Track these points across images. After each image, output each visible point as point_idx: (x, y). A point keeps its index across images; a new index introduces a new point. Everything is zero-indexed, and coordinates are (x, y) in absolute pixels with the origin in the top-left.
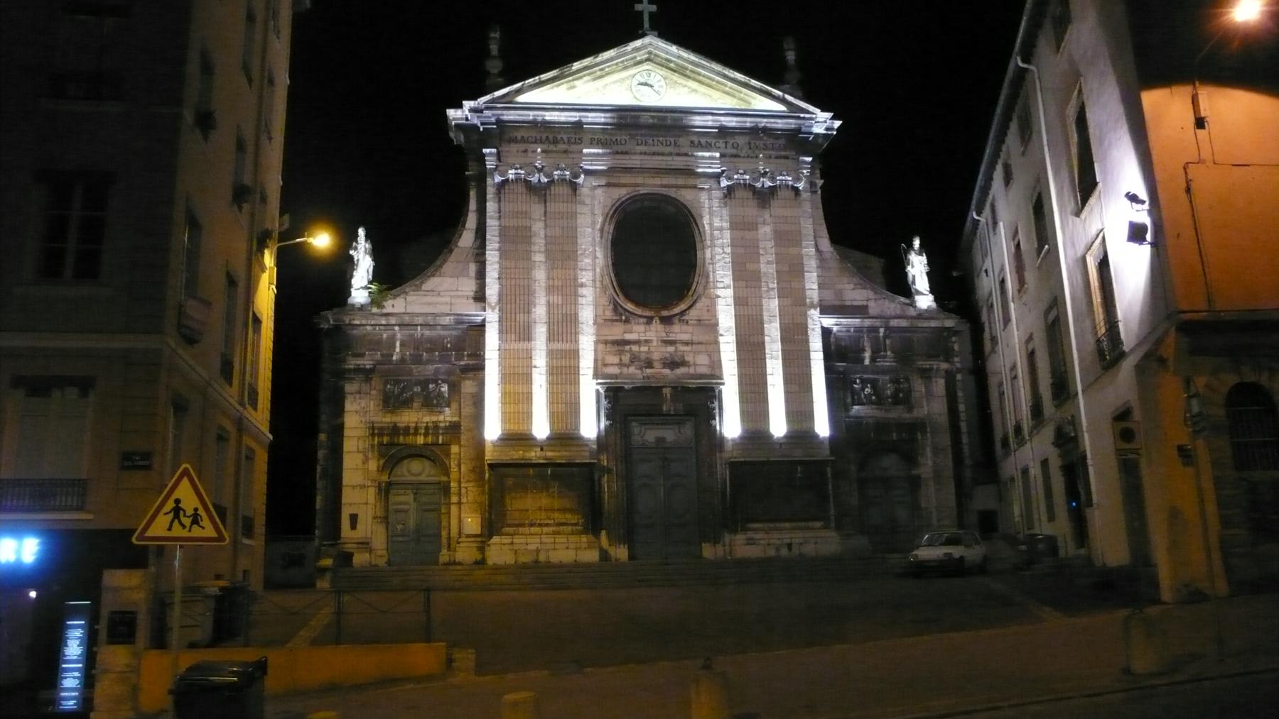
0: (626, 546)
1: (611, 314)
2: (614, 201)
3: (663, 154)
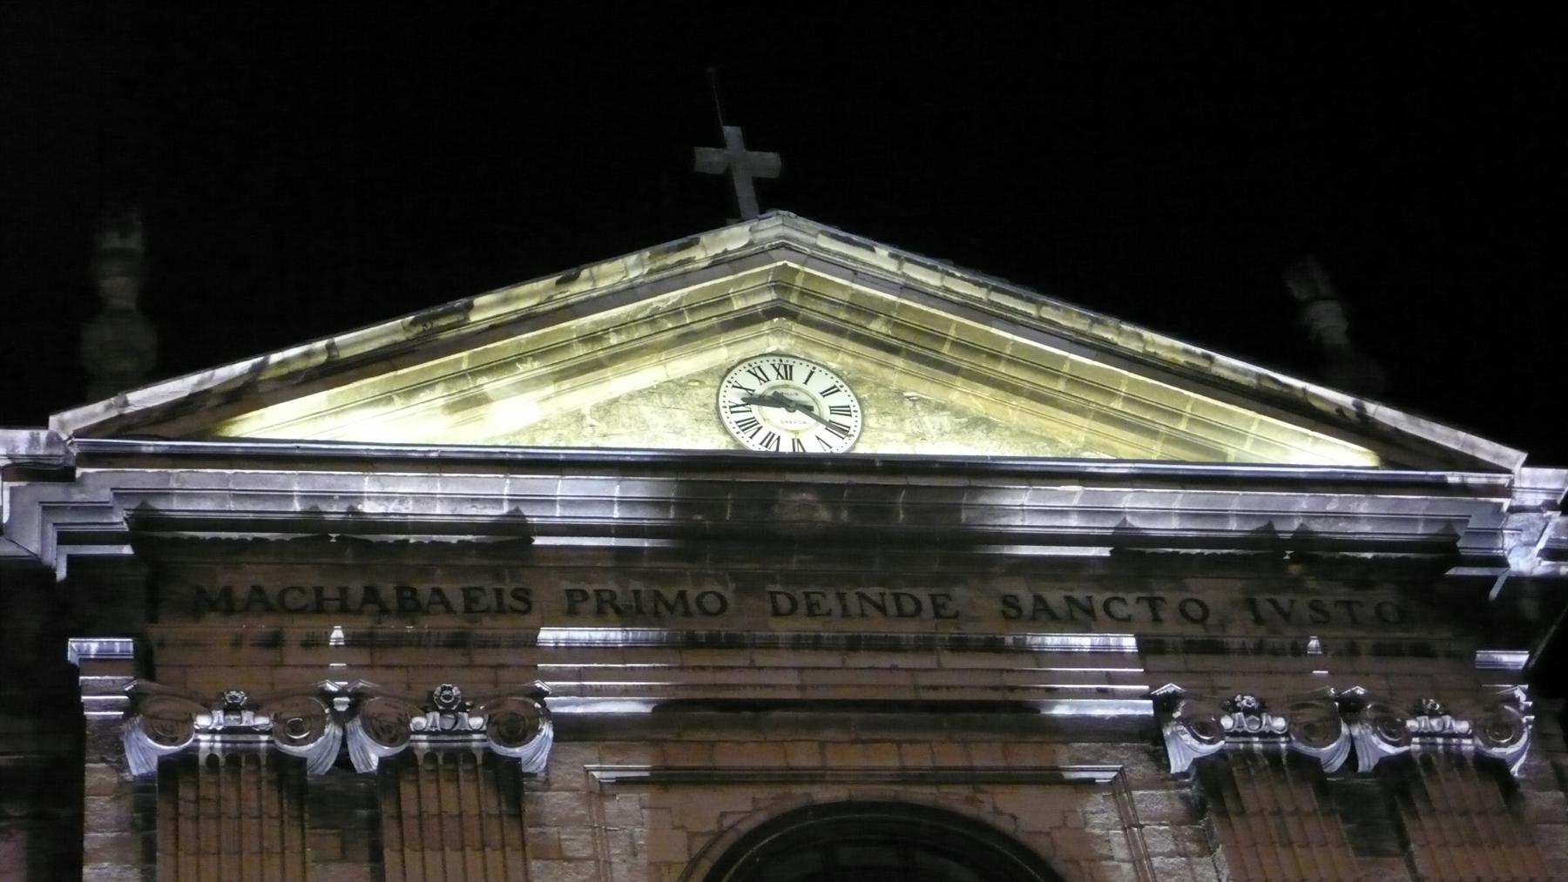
2: (699, 845)
3: (893, 646)
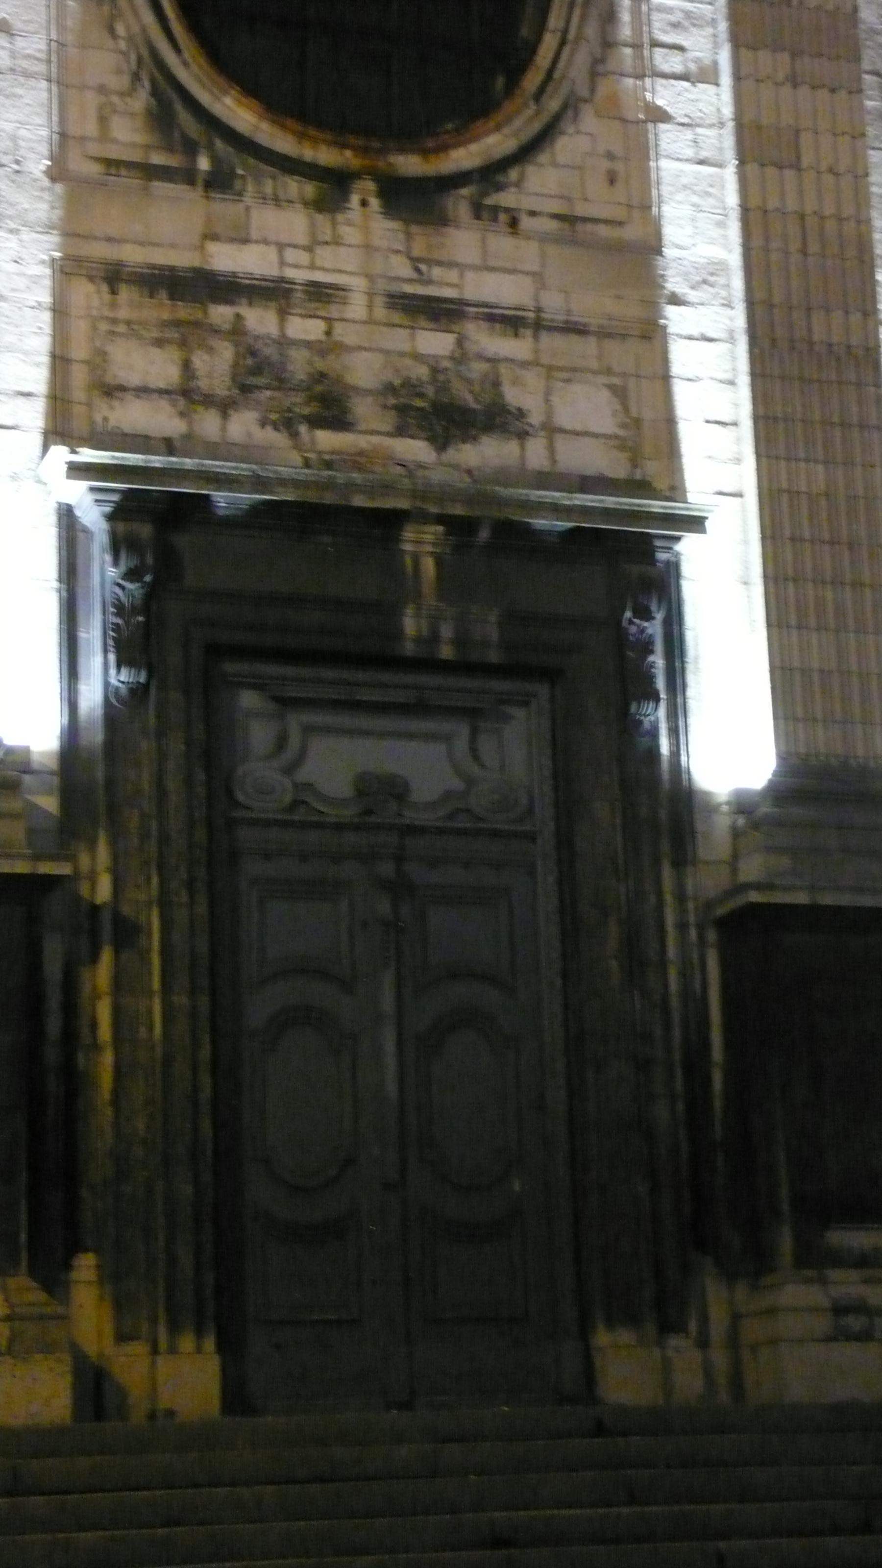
0: (210, 1344)
1: (140, 138)
